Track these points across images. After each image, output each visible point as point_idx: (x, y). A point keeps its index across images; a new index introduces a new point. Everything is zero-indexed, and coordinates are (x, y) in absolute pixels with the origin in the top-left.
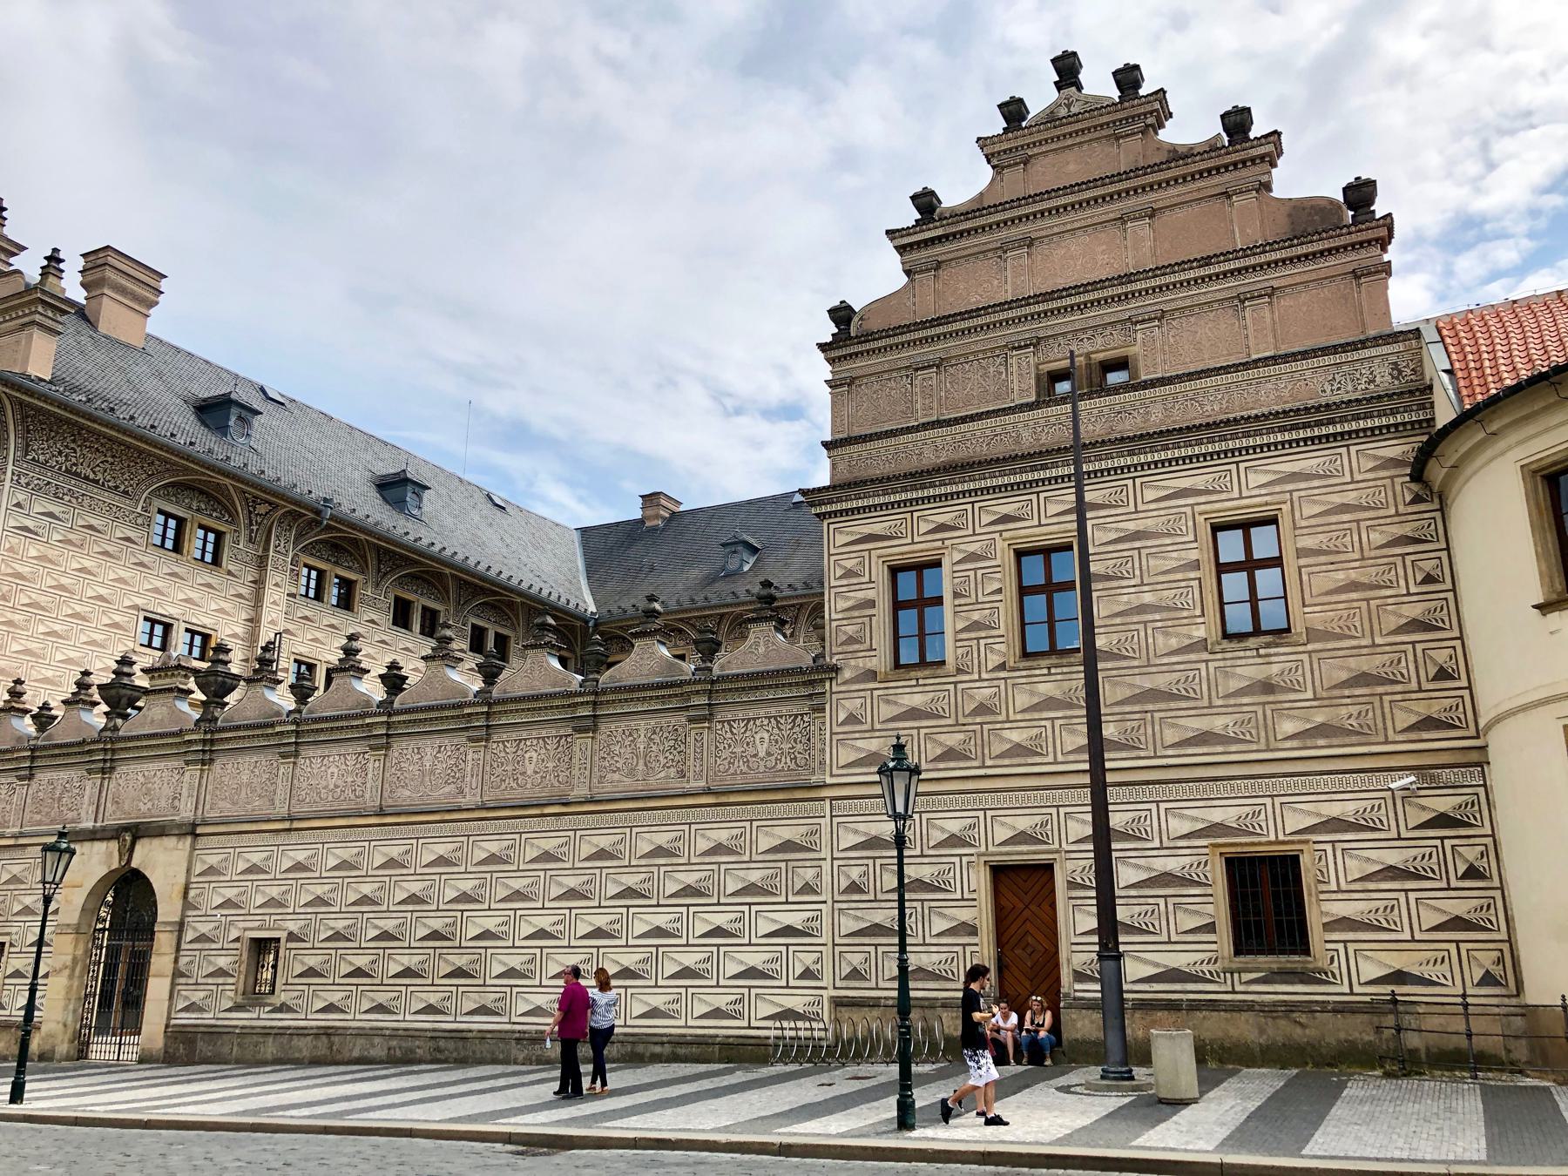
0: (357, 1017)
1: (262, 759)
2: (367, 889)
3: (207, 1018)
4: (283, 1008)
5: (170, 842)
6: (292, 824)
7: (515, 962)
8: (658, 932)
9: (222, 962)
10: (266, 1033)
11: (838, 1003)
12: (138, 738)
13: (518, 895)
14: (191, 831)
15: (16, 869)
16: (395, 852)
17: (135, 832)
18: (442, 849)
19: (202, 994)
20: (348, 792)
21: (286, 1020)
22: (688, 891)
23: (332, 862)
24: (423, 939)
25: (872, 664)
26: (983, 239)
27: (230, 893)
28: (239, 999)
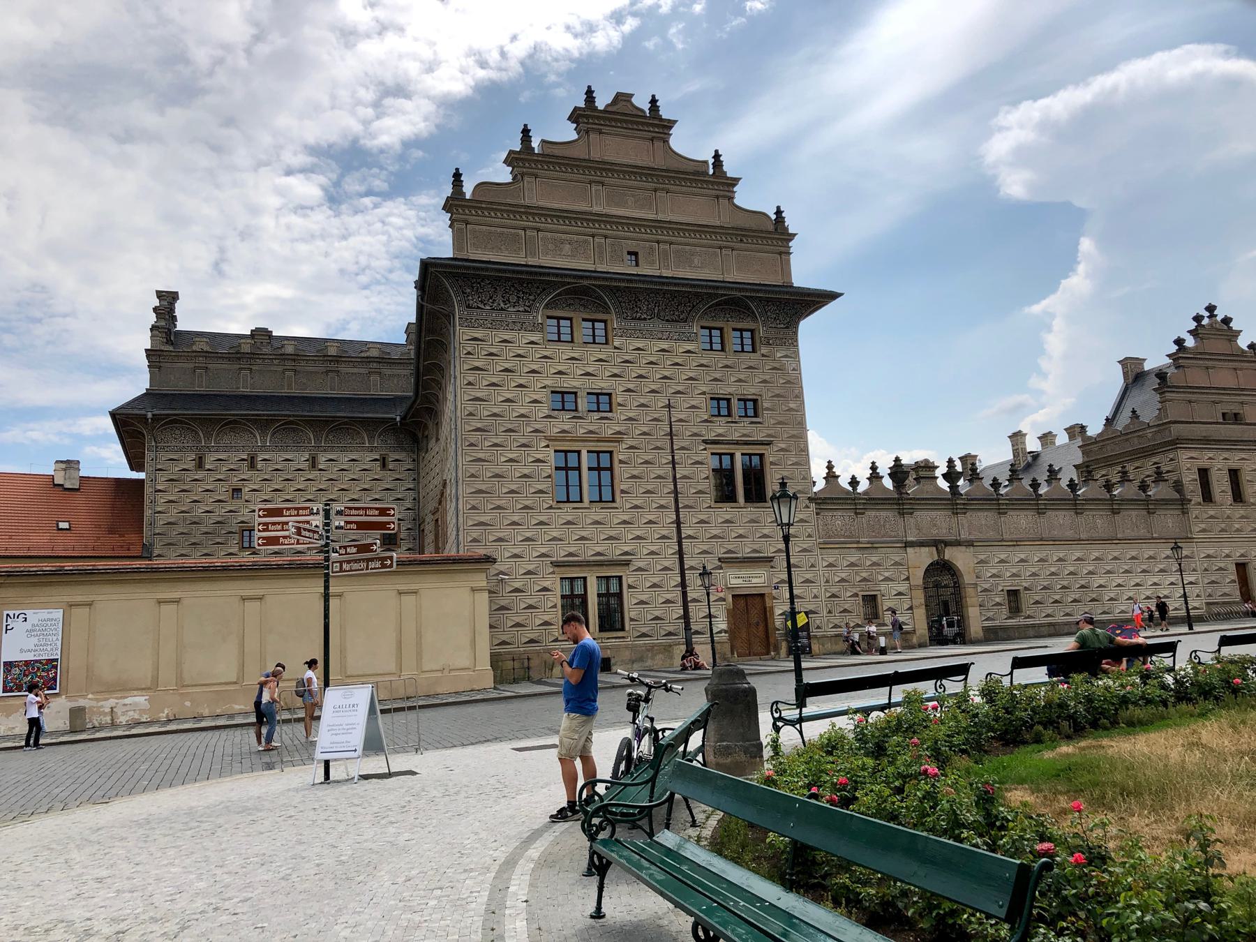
0: (1059, 618)
1: (989, 514)
2: (1053, 570)
3: (997, 623)
4: (1029, 617)
5: (963, 548)
6: (1016, 543)
7: (1112, 595)
8: (1155, 584)
9: (998, 600)
10: (1027, 626)
11: (1208, 604)
12: (923, 499)
13: (1109, 572)
14: (970, 544)
15: (874, 559)
16: (1061, 555)
17: (939, 544)
18: (1078, 554)
19: (992, 613)
20: (1032, 530)
21: (1030, 621)
22: (1162, 571)
23: (1036, 559)
24: (1151, 585)
25: (1199, 500)
26: (1202, 362)
27: (994, 571)
28: (1009, 615)
